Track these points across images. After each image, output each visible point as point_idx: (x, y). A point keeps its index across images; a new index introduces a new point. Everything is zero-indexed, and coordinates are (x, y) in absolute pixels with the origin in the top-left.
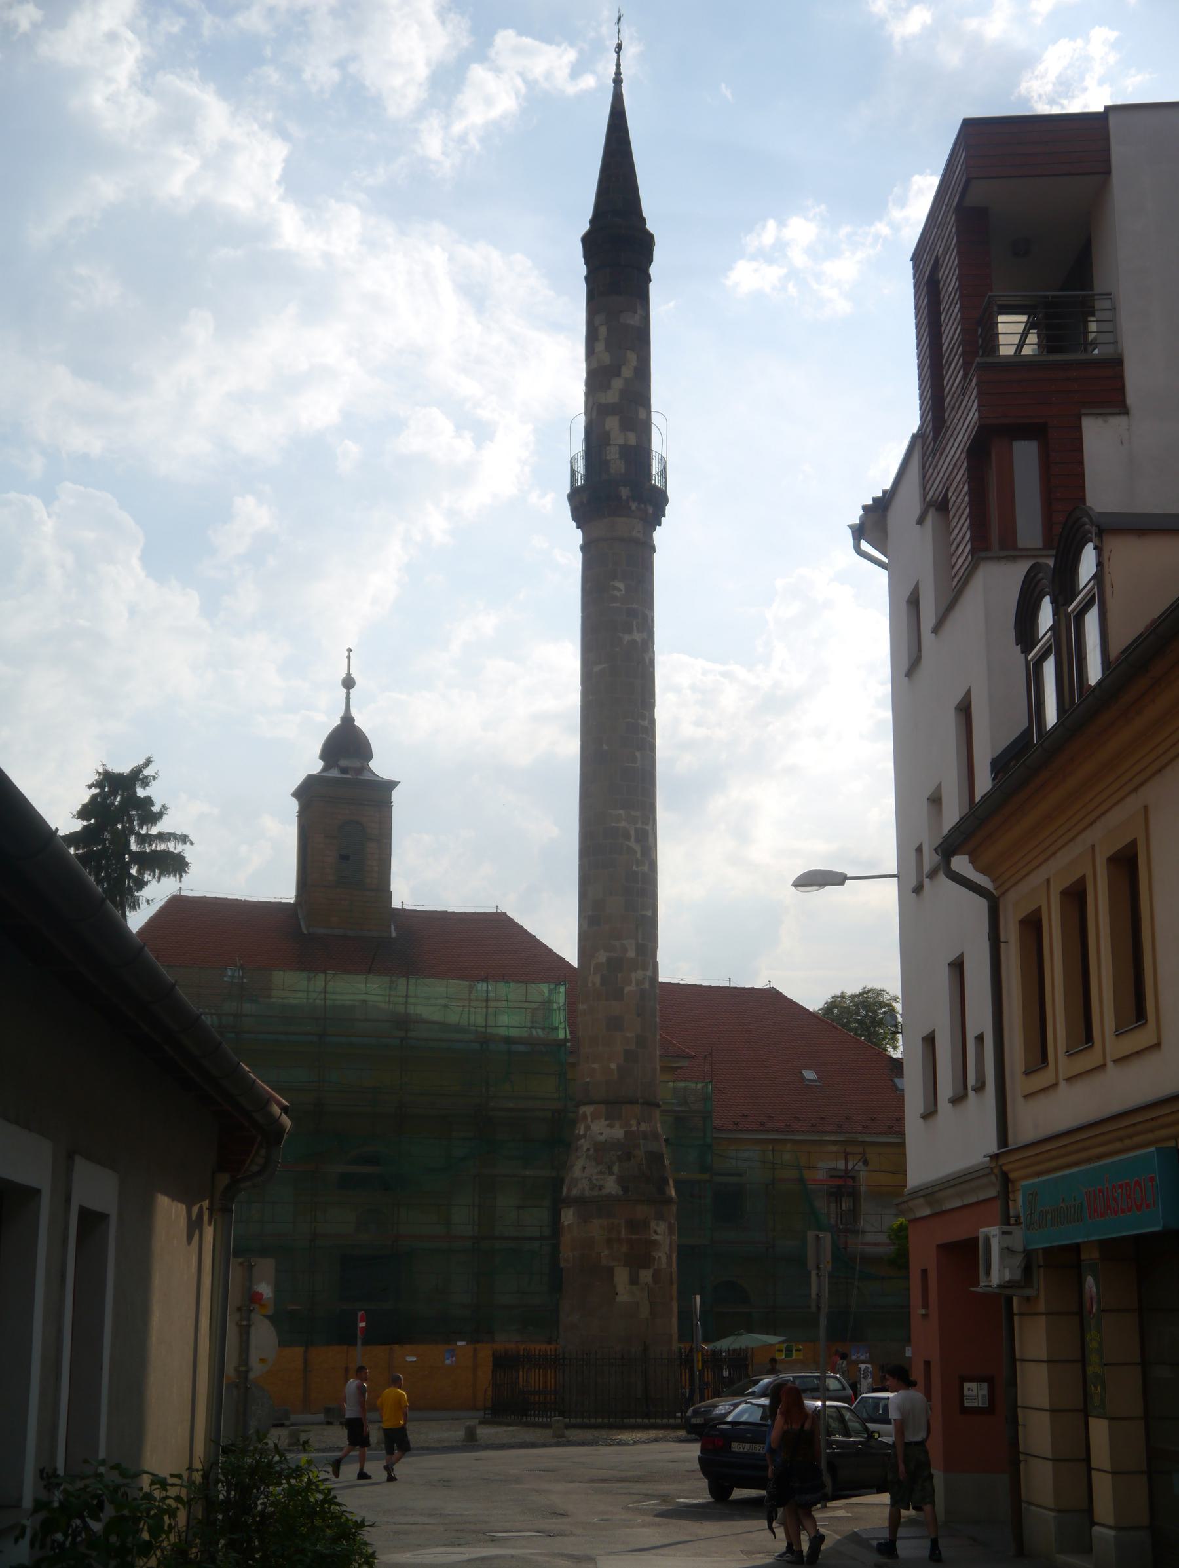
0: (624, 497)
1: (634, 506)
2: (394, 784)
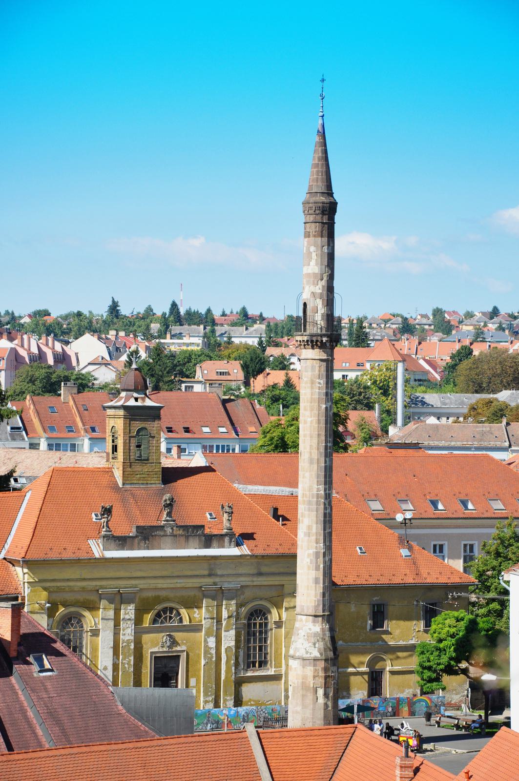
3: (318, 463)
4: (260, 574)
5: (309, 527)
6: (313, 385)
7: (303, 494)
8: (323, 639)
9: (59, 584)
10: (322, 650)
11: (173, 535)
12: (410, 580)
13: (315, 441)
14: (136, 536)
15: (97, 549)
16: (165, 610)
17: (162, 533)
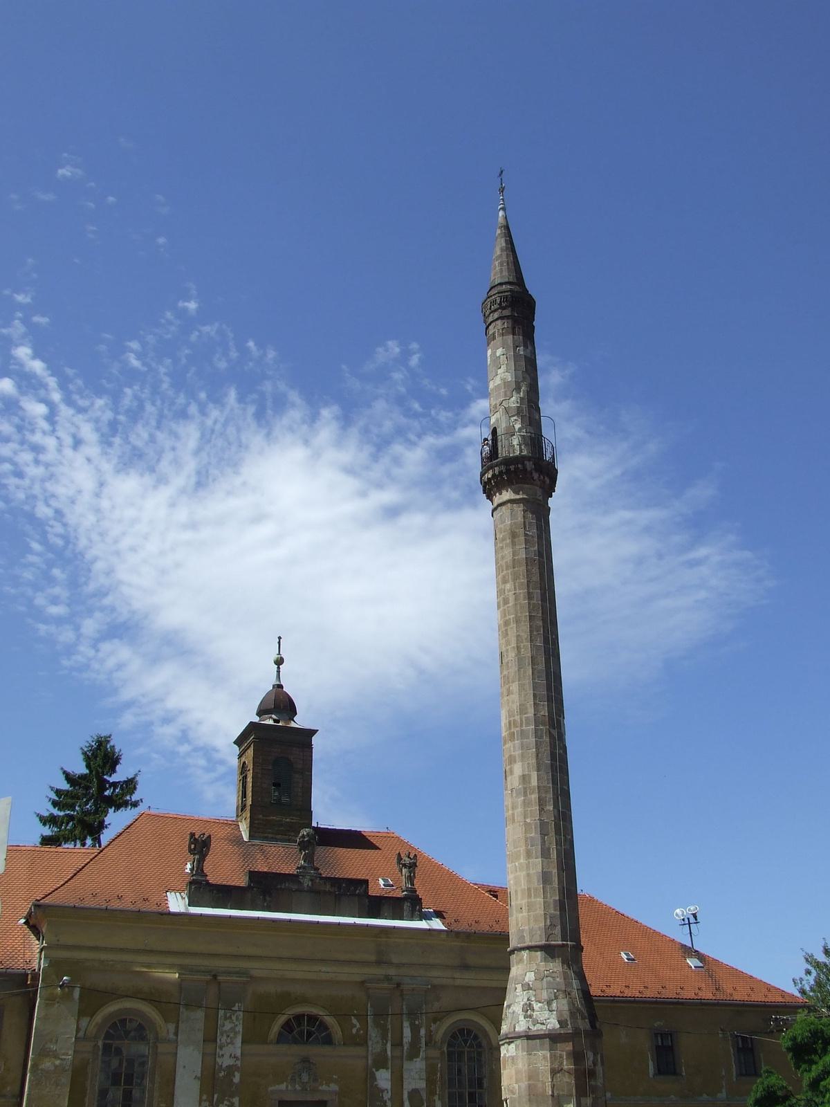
0: (529, 469)
1: (536, 476)
2: (313, 732)
3: (533, 664)
4: (465, 967)
5: (525, 778)
6: (516, 540)
7: (510, 722)
8: (567, 994)
9: (103, 956)
10: (566, 1015)
11: (311, 891)
12: (707, 995)
13: (525, 627)
14: (249, 888)
15: (177, 903)
16: (299, 1018)
17: (294, 887)
